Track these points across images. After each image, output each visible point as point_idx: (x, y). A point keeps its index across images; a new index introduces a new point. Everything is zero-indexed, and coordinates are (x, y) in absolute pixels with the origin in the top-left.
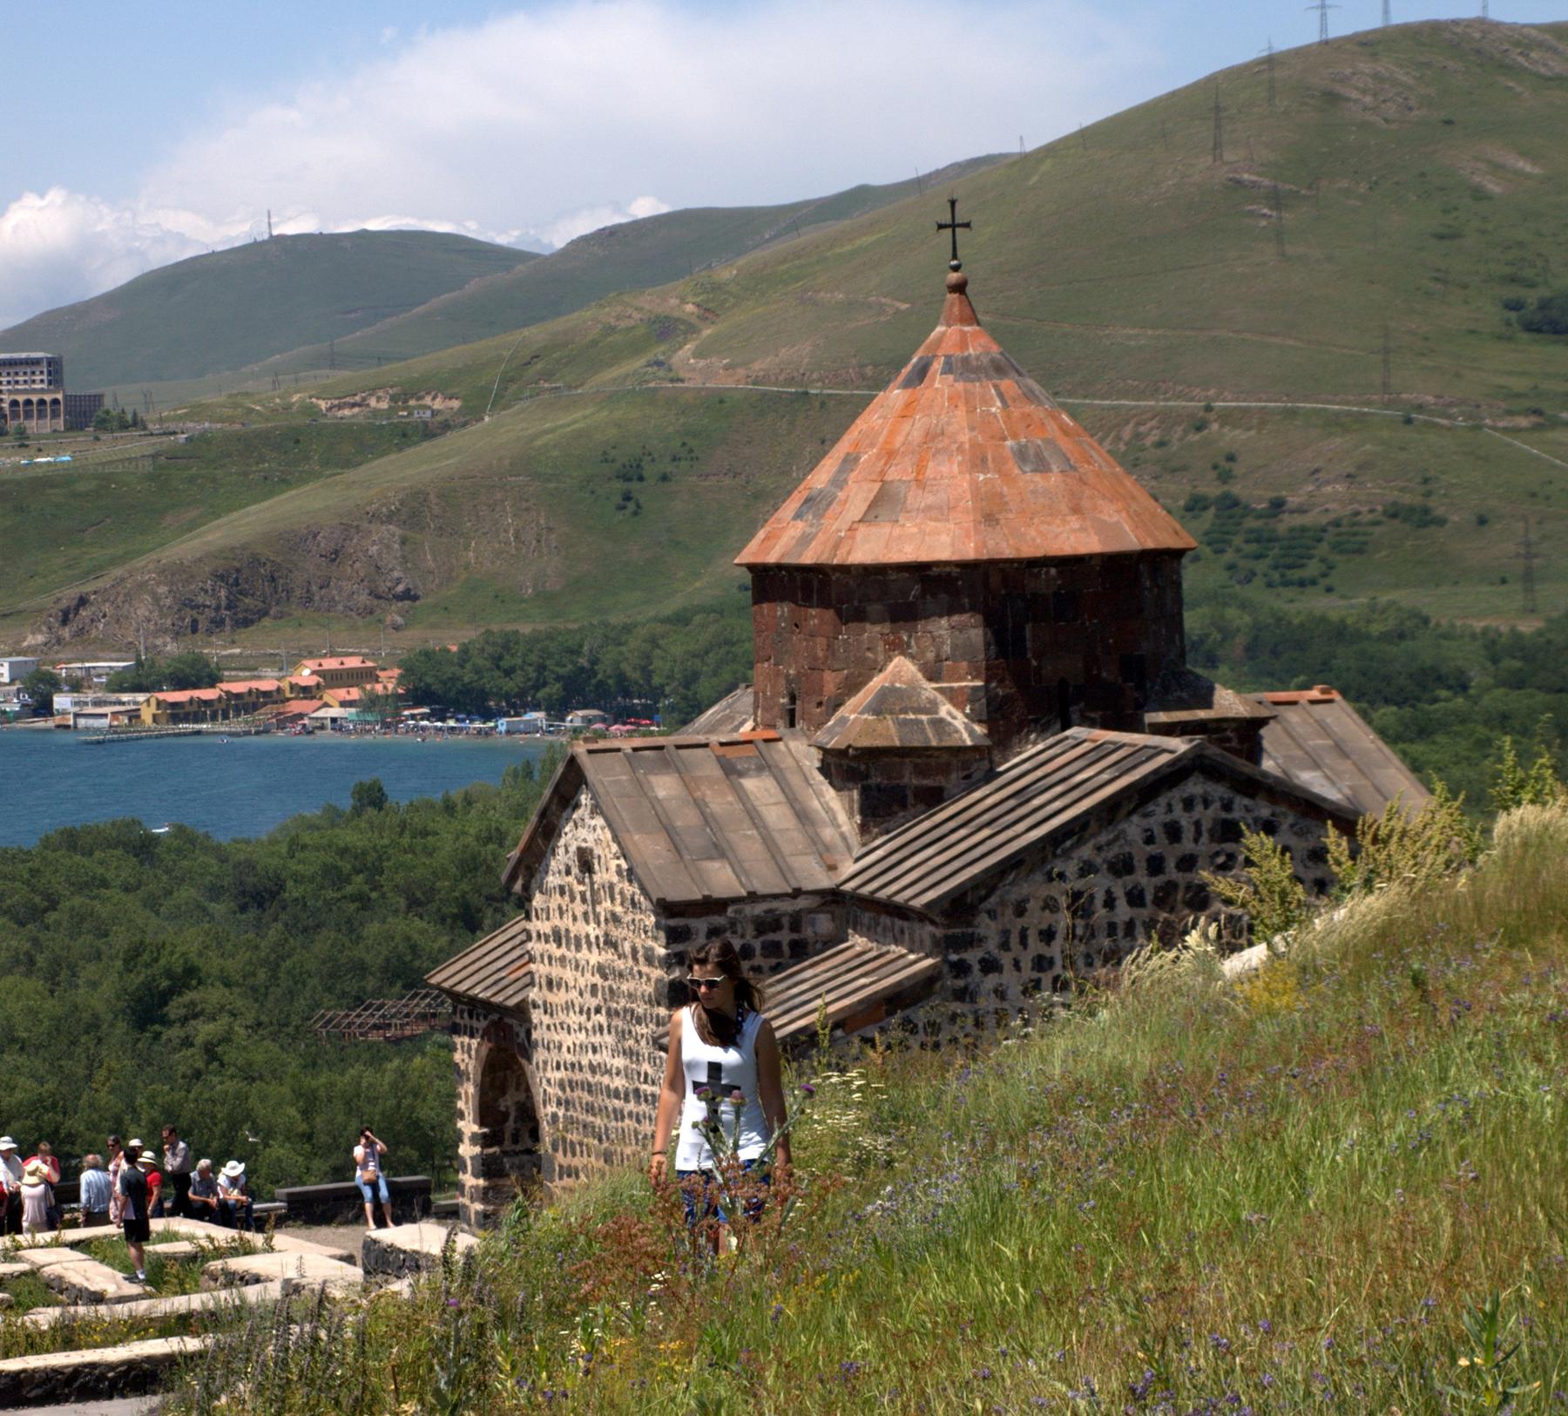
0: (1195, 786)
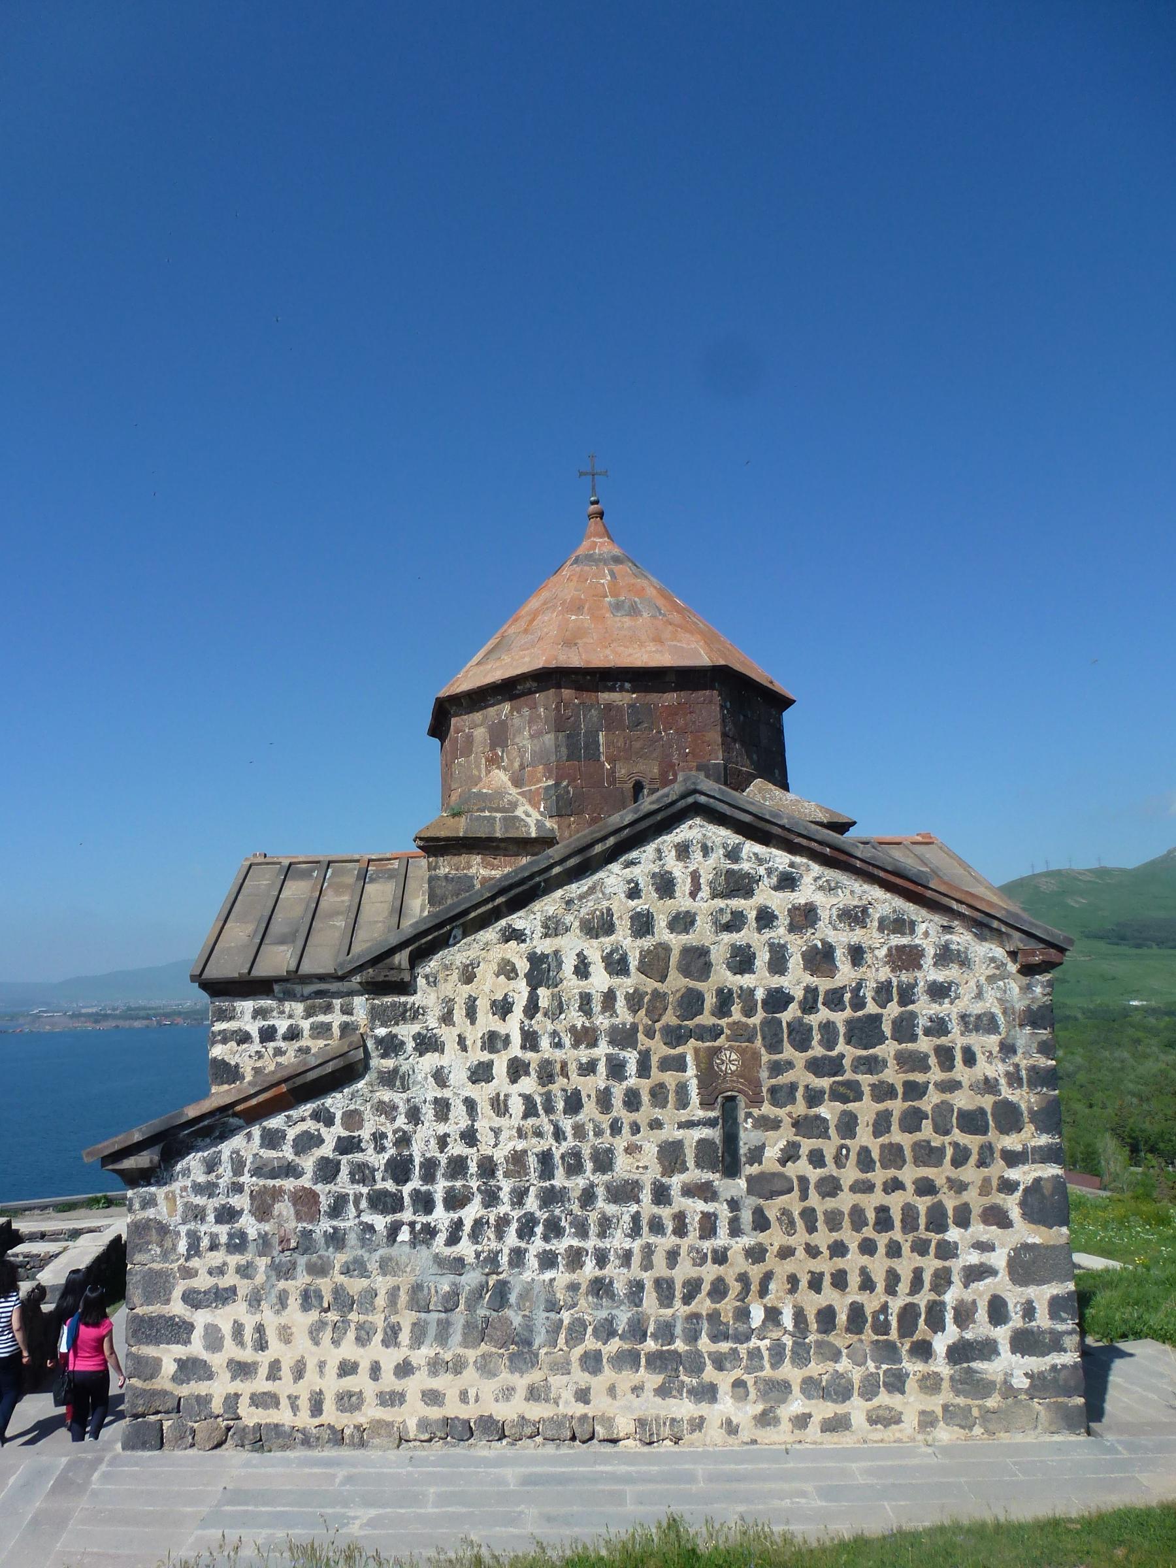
0: (691, 831)
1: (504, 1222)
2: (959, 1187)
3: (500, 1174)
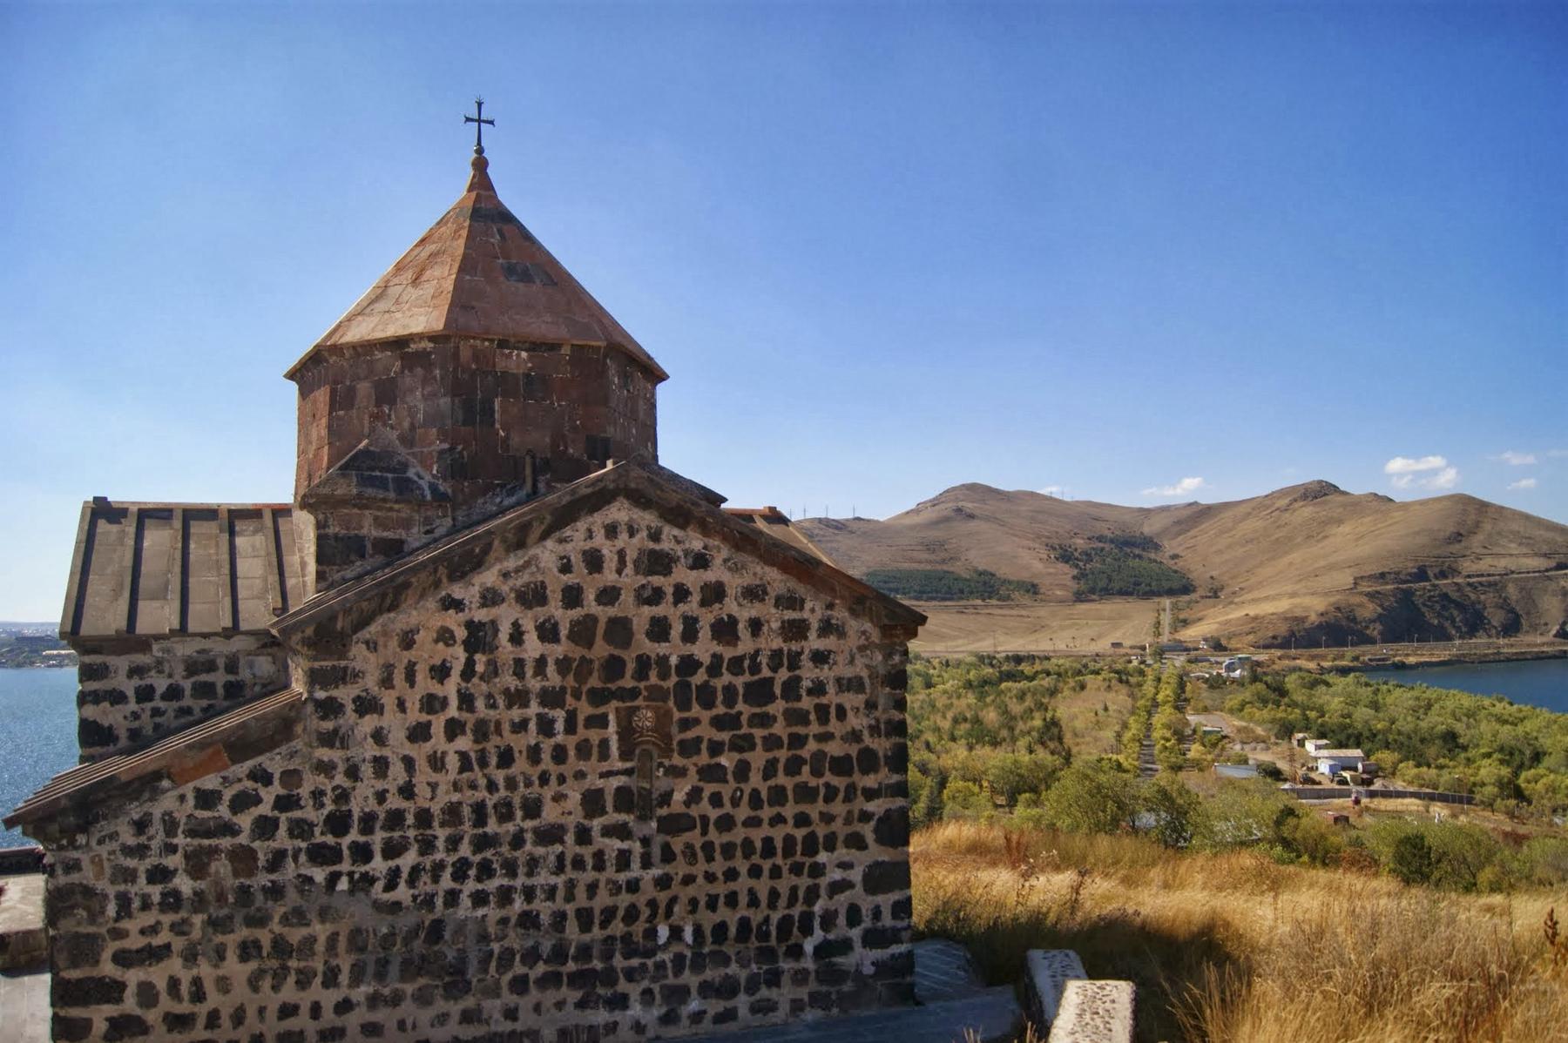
0: (619, 512)
1: (439, 867)
2: (828, 818)
3: (436, 824)
